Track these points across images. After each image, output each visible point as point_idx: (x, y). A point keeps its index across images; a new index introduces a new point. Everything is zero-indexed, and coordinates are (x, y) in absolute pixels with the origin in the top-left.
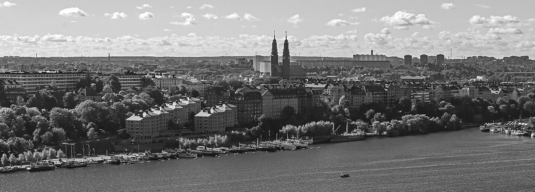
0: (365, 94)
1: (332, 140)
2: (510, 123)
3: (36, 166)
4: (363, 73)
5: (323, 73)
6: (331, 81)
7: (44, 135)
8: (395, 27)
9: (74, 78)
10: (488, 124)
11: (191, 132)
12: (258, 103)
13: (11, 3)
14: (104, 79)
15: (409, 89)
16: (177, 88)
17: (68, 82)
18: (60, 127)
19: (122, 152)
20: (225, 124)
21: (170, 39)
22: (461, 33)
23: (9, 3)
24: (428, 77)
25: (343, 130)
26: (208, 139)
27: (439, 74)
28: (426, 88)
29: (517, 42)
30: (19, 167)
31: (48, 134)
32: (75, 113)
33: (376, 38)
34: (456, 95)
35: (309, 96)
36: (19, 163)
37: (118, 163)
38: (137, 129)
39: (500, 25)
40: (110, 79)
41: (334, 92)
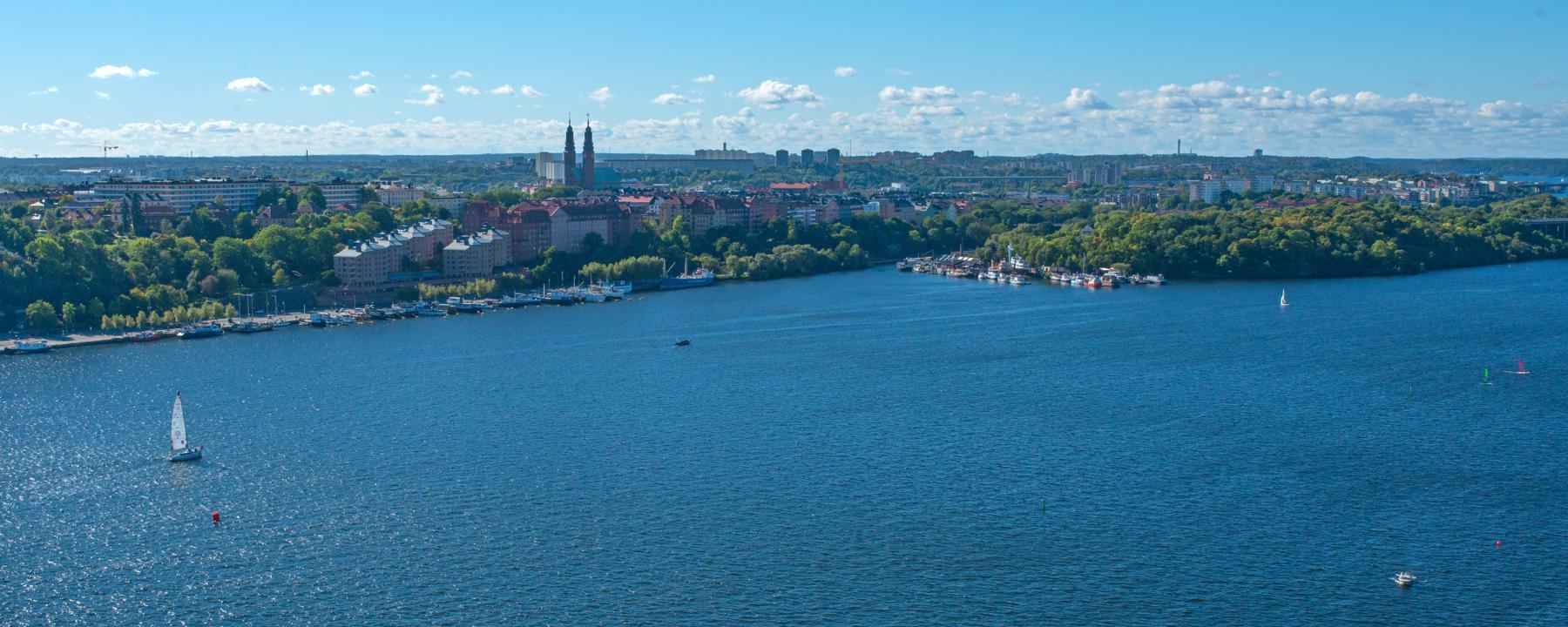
0: (714, 213)
1: (662, 287)
2: (945, 258)
3: (192, 330)
4: (710, 179)
5: (648, 179)
6: (660, 193)
7: (204, 282)
8: (760, 106)
9: (251, 191)
10: (910, 260)
11: (437, 274)
12: (545, 228)
13: (151, 70)
14: (299, 190)
15: (784, 203)
16: (416, 205)
17: (242, 196)
18: (229, 268)
19: (329, 307)
20: (492, 262)
21: (403, 126)
22: (866, 115)
23: (148, 71)
24: (815, 184)
25: (679, 270)
26: (465, 286)
27: (832, 180)
28: (812, 203)
29: (955, 128)
30: (164, 331)
31: (212, 280)
32: (253, 245)
33: (730, 123)
34: (858, 213)
35: (625, 215)
36: (165, 326)
37: (320, 324)
38: (352, 270)
39: (928, 101)
40: (309, 191)
41: (665, 210)
